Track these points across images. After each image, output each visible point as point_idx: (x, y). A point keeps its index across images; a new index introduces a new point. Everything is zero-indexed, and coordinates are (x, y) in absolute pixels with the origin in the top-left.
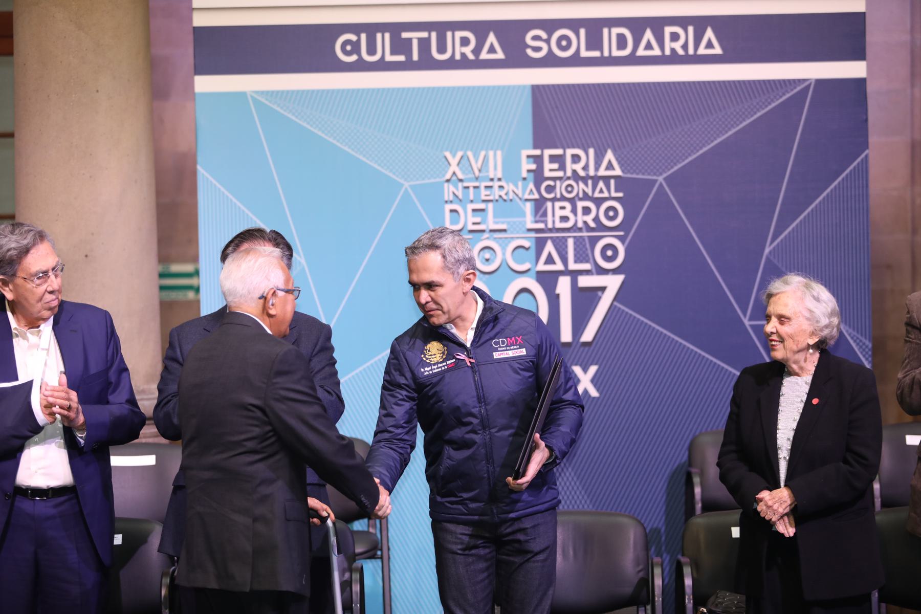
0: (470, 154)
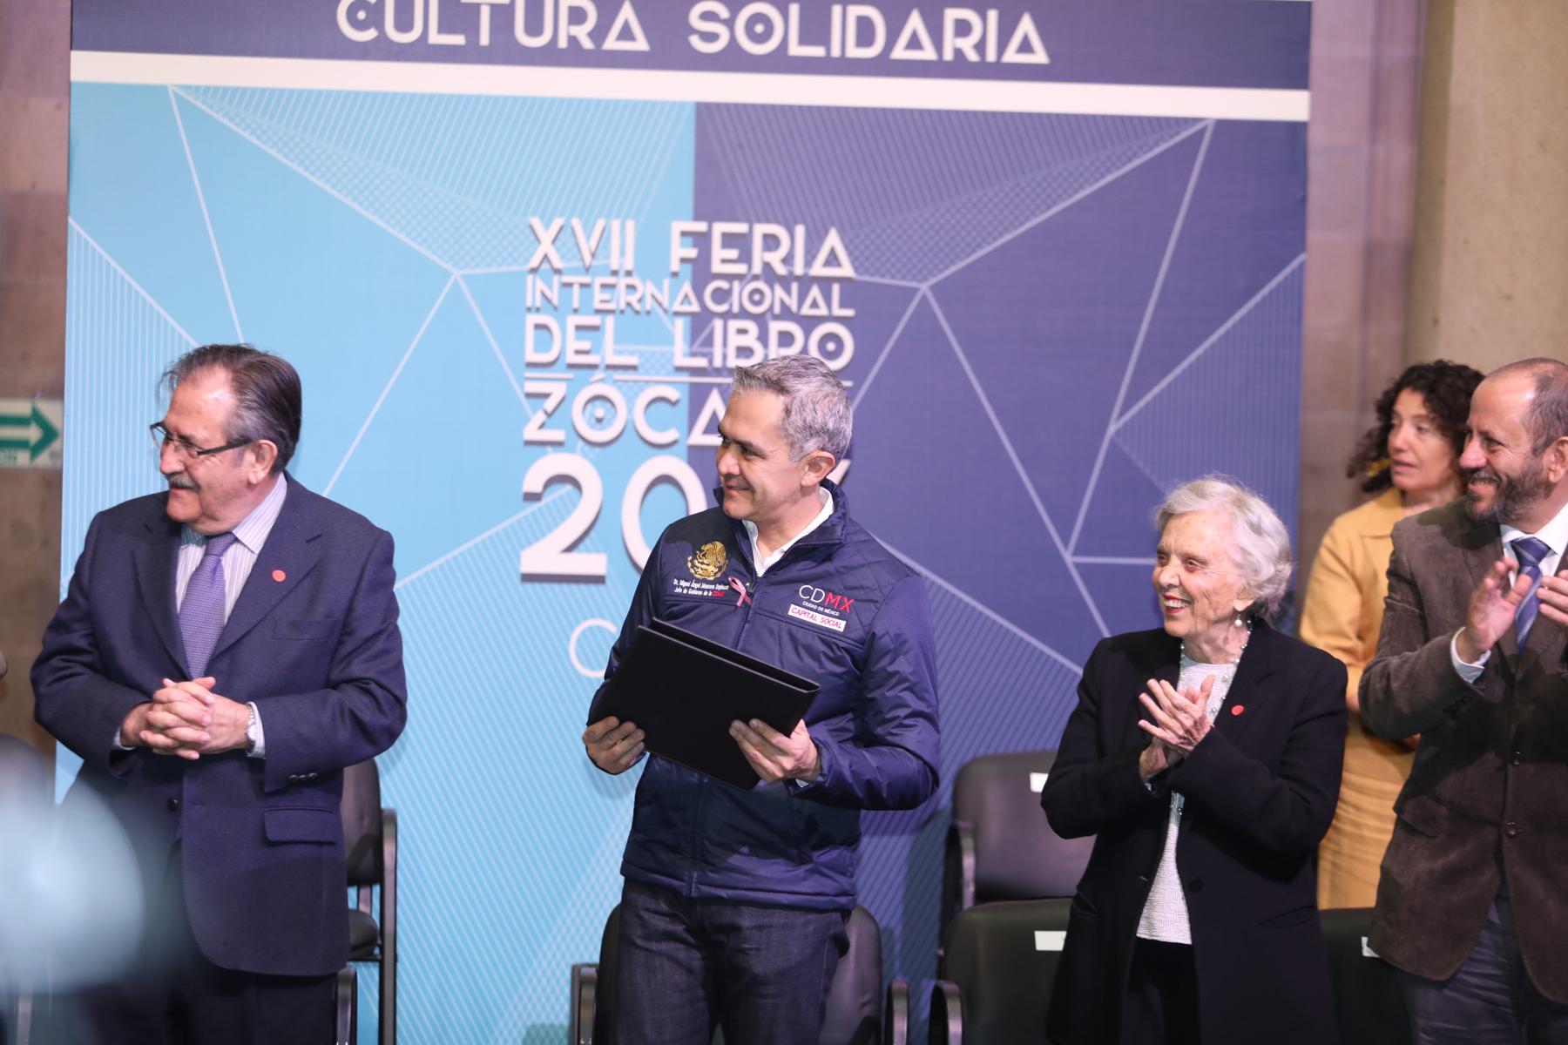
0: (576, 223)
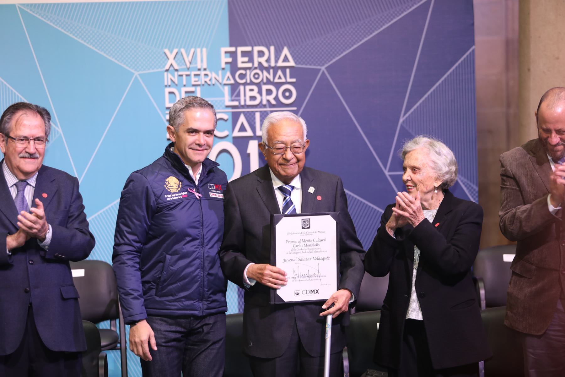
0: (183, 51)
